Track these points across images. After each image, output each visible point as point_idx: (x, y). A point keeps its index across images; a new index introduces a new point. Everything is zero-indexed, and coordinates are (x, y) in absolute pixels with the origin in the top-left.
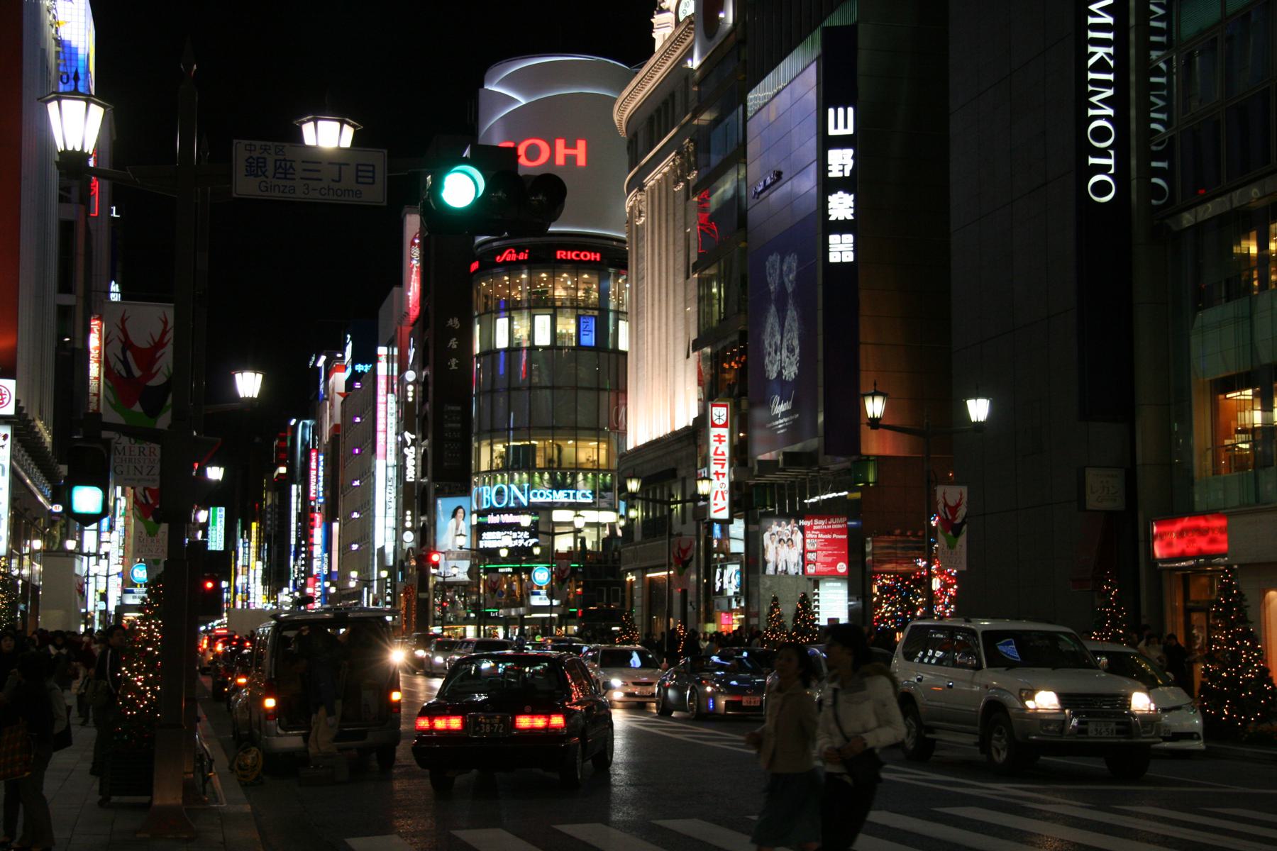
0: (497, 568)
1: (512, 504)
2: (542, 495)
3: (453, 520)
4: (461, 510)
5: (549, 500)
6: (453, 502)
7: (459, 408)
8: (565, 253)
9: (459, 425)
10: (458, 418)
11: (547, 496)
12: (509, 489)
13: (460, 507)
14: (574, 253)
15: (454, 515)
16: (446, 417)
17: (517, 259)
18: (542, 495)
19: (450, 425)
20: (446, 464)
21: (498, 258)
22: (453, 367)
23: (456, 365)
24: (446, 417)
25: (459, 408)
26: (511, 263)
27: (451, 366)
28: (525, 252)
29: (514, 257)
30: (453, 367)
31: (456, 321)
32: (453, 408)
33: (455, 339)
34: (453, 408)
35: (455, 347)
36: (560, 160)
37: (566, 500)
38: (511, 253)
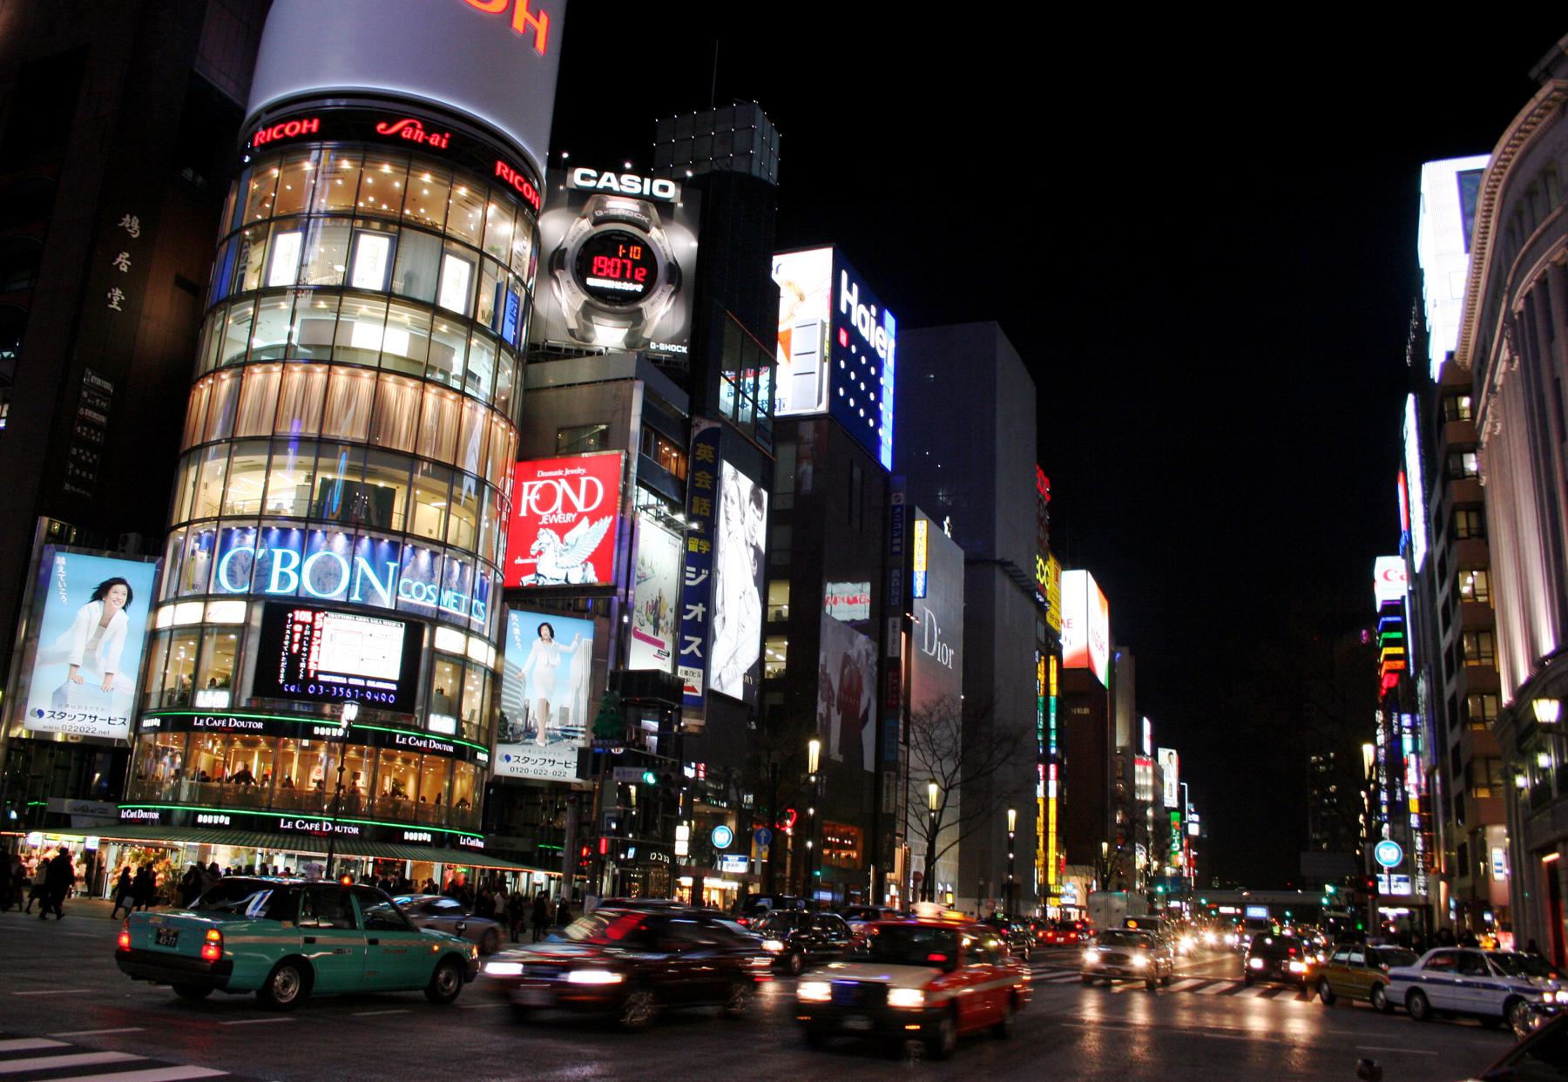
0: (313, 725)
1: (356, 598)
2: (419, 591)
3: (96, 603)
4: (120, 589)
5: (431, 604)
6: (102, 568)
7: (107, 386)
8: (507, 170)
9: (103, 419)
11: (428, 597)
12: (353, 565)
13: (121, 581)
14: (518, 178)
15: (101, 593)
16: (85, 394)
17: (426, 142)
18: (419, 591)
19: (89, 413)
20: (67, 486)
21: (381, 126)
22: (115, 305)
23: (120, 303)
25: (107, 386)
26: (411, 143)
27: (111, 301)
28: (443, 136)
29: (419, 135)
30: (115, 305)
31: (135, 223)
33: (127, 255)
36: (518, 24)
37: (452, 610)
38: (414, 126)
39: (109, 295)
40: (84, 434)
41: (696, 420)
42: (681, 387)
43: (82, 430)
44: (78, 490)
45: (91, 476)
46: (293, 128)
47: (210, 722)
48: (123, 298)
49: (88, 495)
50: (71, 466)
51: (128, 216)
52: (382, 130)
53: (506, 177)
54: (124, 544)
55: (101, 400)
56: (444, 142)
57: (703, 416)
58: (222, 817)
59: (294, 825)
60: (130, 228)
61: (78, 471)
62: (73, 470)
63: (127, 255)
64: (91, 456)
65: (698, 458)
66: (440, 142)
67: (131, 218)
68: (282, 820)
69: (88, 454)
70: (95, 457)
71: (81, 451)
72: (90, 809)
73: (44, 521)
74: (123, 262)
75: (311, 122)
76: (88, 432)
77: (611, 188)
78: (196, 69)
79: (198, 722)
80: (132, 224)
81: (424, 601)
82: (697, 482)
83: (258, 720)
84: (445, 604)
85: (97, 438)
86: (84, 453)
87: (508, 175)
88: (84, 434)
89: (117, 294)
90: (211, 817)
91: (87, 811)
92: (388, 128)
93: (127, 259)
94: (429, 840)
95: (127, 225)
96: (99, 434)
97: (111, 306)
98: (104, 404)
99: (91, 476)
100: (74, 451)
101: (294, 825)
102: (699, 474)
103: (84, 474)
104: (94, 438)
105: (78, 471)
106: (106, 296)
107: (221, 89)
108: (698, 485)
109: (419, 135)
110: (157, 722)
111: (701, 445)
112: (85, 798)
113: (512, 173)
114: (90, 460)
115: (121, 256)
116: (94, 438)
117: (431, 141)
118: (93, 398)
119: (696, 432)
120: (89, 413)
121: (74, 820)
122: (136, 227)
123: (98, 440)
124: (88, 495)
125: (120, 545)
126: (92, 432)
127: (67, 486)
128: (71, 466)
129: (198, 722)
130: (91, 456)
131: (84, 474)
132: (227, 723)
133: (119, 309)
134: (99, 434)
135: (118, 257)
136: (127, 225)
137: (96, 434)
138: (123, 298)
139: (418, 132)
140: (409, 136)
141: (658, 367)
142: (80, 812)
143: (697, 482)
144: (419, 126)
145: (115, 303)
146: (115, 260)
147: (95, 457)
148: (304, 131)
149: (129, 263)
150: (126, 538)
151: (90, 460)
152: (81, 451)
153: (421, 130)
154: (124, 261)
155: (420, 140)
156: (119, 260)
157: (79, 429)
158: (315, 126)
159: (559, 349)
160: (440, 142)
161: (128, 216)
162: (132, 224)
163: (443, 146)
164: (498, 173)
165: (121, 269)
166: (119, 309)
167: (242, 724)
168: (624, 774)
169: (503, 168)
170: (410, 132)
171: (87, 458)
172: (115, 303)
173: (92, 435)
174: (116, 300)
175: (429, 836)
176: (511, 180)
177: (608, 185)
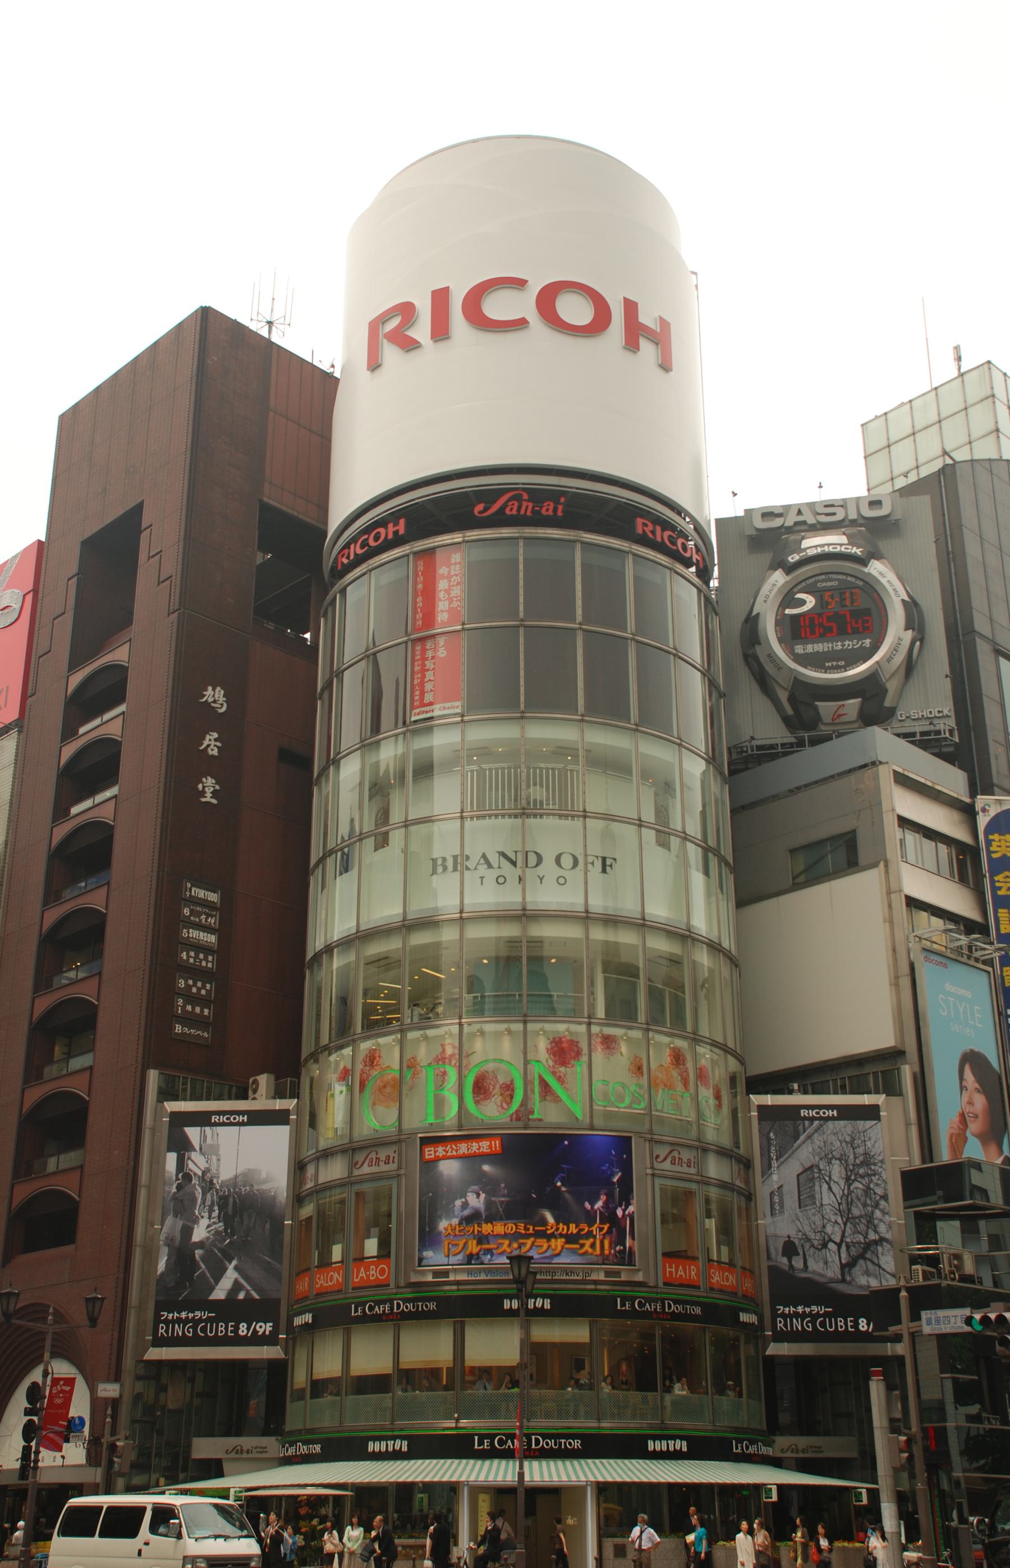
7: (213, 897)
8: (650, 527)
9: (212, 939)
10: (212, 921)
14: (667, 533)
16: (186, 911)
19: (194, 934)
20: (178, 1028)
23: (215, 794)
24: (186, 911)
25: (213, 897)
27: (203, 793)
30: (208, 798)
32: (201, 893)
33: (216, 735)
34: (201, 893)
35: (215, 752)
39: (200, 786)
40: (191, 960)
41: (981, 800)
42: (954, 765)
43: (189, 957)
44: (193, 1031)
45: (206, 1012)
46: (376, 539)
47: (371, 1308)
48: (218, 787)
49: (206, 1035)
50: (180, 1002)
51: (210, 688)
52: (480, 513)
53: (651, 536)
54: (255, 1091)
55: (208, 915)
56: (560, 508)
57: (988, 790)
58: (398, 1442)
59: (492, 1444)
60: (215, 702)
61: (189, 1008)
62: (184, 1007)
63: (216, 735)
64: (204, 987)
65: (994, 856)
66: (555, 510)
67: (214, 690)
68: (476, 1438)
69: (199, 984)
70: (208, 986)
71: (190, 982)
72: (245, 1449)
73: (153, 1076)
74: (211, 743)
75: (396, 524)
76: (196, 957)
77: (804, 523)
78: (265, 499)
79: (356, 1311)
80: (215, 696)
81: (630, 1107)
82: (1000, 888)
83: (430, 1299)
84: (659, 1107)
85: (209, 963)
86: (195, 985)
87: (653, 532)
88: (191, 960)
89: (209, 784)
90: (383, 1443)
91: (242, 1452)
92: (486, 510)
93: (216, 740)
94: (685, 1449)
95: (211, 700)
96: (210, 958)
97: (203, 800)
98: (212, 921)
99: (206, 1012)
100: (182, 983)
101: (492, 1444)
102: (999, 877)
103: (198, 1010)
104: (204, 964)
105: (189, 1008)
106: (197, 789)
107: (301, 516)
108: (999, 893)
109: (527, 506)
110: (308, 1318)
111: (996, 837)
112: (239, 1434)
113: (658, 529)
114: (203, 992)
115: (208, 737)
116: (204, 964)
117: (544, 512)
118: (199, 914)
119: (983, 821)
120: (194, 934)
121: (226, 1467)
122: (222, 699)
123: (210, 965)
124: (206, 1035)
125: (250, 1093)
126: (201, 956)
127: (178, 1028)
128: (180, 1002)
129: (356, 1311)
130: (204, 987)
131: (198, 1010)
132: (392, 1308)
133: (214, 801)
134: (210, 958)
135: (204, 739)
136: (211, 700)
137: (206, 959)
138: (218, 787)
139: (525, 504)
140: (514, 512)
141: (913, 743)
142: (233, 1455)
143: (1000, 888)
144: (525, 496)
145: (209, 795)
146: (202, 744)
147: (208, 986)
148: (390, 536)
149: (219, 744)
150: (256, 1082)
151: (203, 992)
152: (190, 982)
153: (528, 501)
154: (213, 743)
155: (529, 514)
156: (206, 743)
157: (184, 956)
158: (401, 527)
159: (772, 747)
160: (555, 510)
161: (210, 688)
162: (215, 696)
163: (560, 513)
164: (639, 531)
165: (210, 752)
166: (214, 801)
167: (410, 1306)
168: (938, 1321)
169: (645, 525)
170: (515, 508)
171: (199, 990)
172: (209, 795)
173: (201, 960)
174: (209, 791)
175: (685, 1443)
176: (659, 539)
177: (800, 518)
